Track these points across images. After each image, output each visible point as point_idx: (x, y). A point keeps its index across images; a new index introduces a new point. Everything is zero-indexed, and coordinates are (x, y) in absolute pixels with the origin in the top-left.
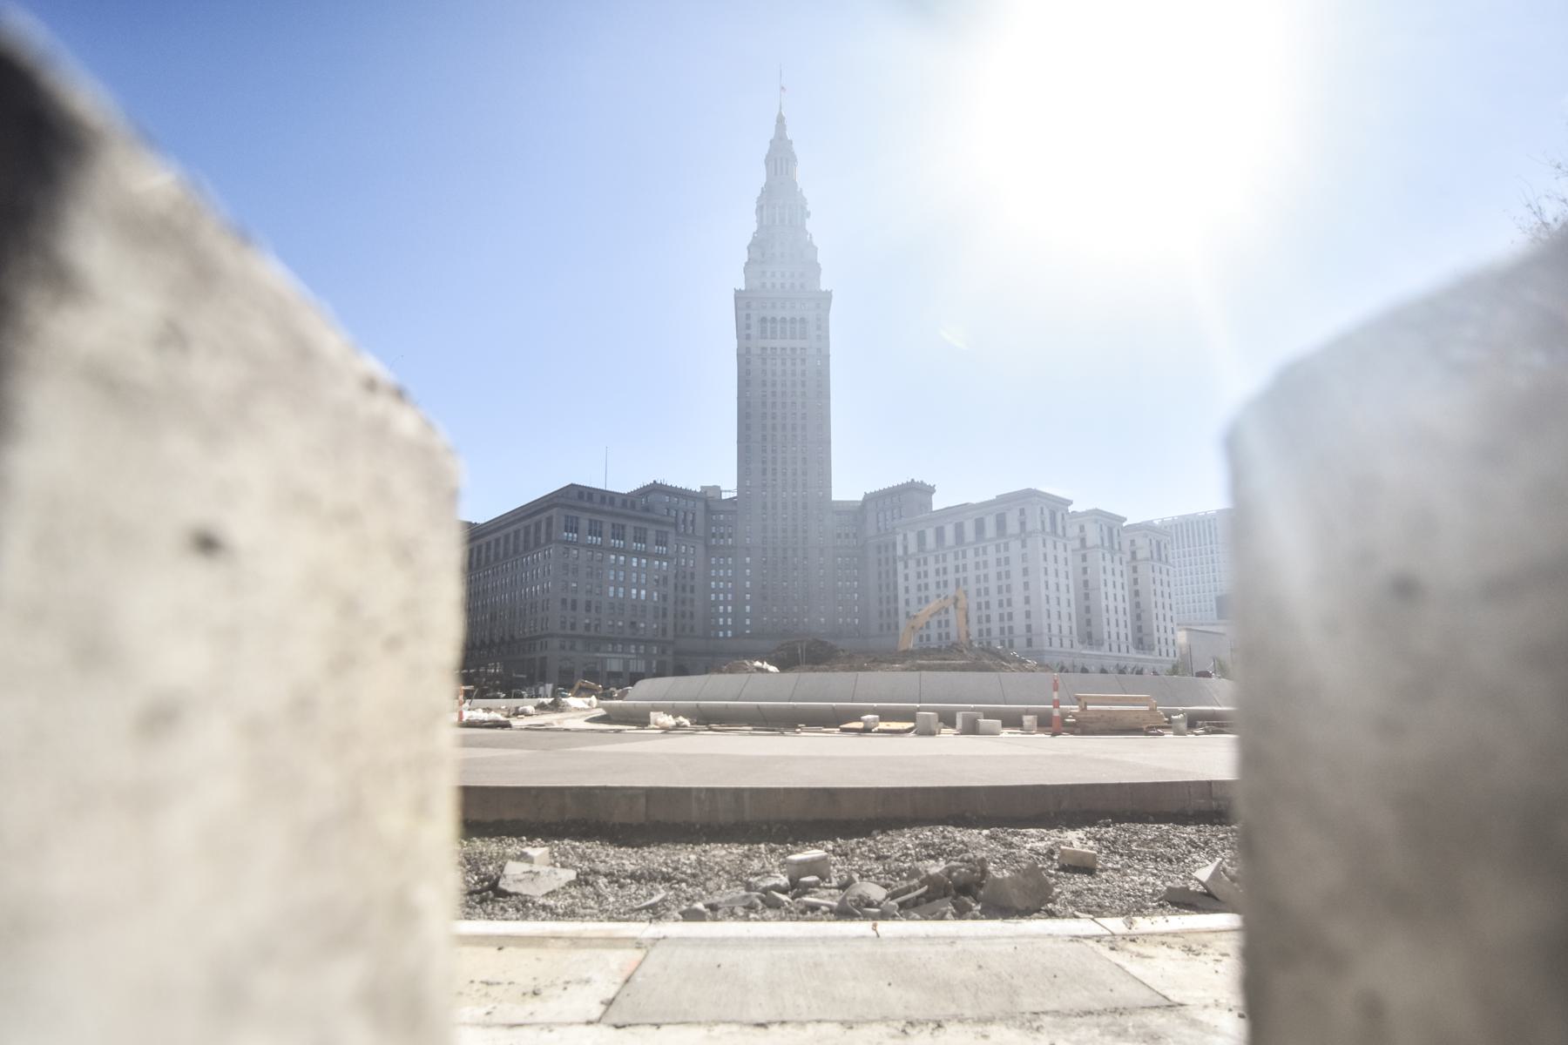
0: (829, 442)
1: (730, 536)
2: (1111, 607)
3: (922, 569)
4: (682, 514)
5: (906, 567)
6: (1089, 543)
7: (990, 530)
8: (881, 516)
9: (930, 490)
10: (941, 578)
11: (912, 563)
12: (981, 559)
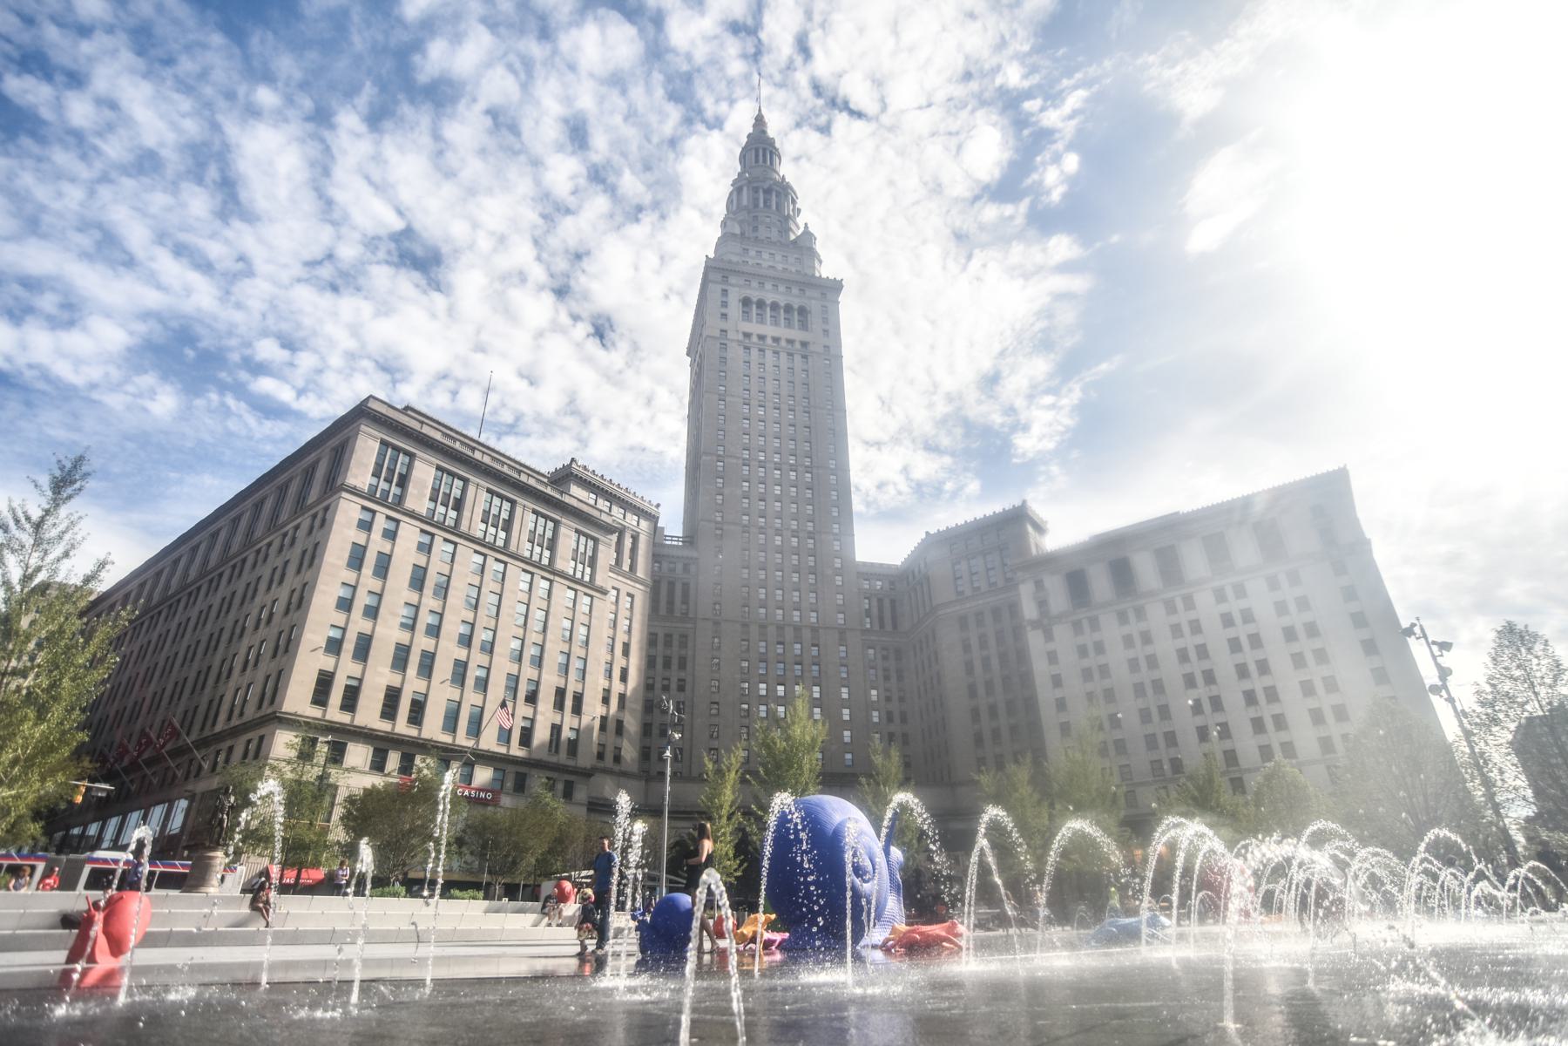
11: (1062, 632)
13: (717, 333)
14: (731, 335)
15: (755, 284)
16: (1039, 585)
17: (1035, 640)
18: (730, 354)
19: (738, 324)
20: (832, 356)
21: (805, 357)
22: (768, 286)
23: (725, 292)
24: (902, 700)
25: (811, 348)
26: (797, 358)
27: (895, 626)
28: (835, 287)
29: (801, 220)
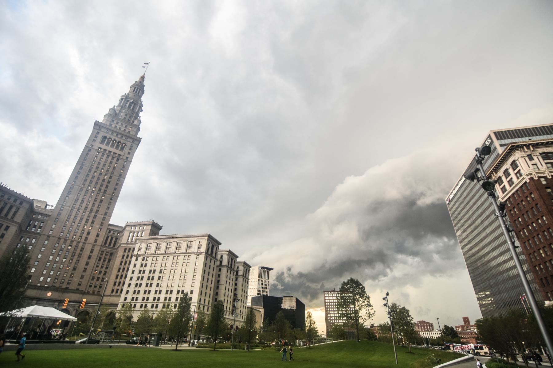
1: (40, 227)
2: (226, 294)
3: (144, 262)
5: (136, 260)
11: (140, 259)
13: (89, 145)
14: (94, 147)
15: (110, 133)
18: (91, 153)
19: (97, 144)
20: (128, 161)
21: (118, 160)
23: (98, 133)
24: (107, 268)
25: (121, 157)
27: (114, 245)
28: (139, 140)
29: (141, 114)
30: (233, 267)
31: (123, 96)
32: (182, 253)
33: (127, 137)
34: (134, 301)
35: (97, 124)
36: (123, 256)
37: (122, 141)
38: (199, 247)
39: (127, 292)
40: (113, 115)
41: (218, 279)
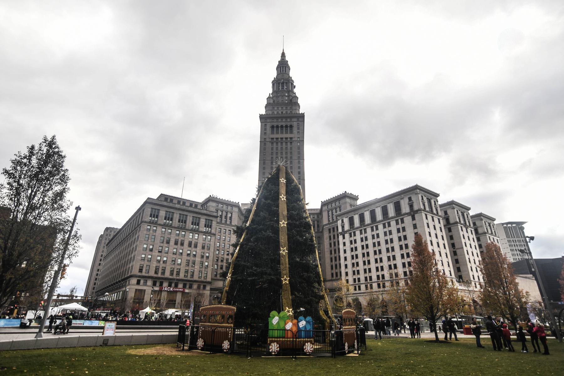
0: (304, 180)
3: (352, 239)
4: (224, 214)
6: (452, 221)
7: (391, 212)
8: (330, 213)
9: (356, 198)
10: (364, 243)
11: (347, 236)
12: (387, 230)
13: (263, 140)
14: (267, 140)
16: (342, 221)
17: (341, 237)
21: (291, 143)
22: (280, 120)
26: (289, 144)
28: (303, 116)
30: (468, 224)
31: (273, 81)
32: (392, 218)
33: (291, 118)
34: (357, 283)
35: (261, 117)
36: (330, 237)
37: (289, 124)
38: (411, 206)
39: (347, 274)
40: (271, 103)
41: (452, 242)
